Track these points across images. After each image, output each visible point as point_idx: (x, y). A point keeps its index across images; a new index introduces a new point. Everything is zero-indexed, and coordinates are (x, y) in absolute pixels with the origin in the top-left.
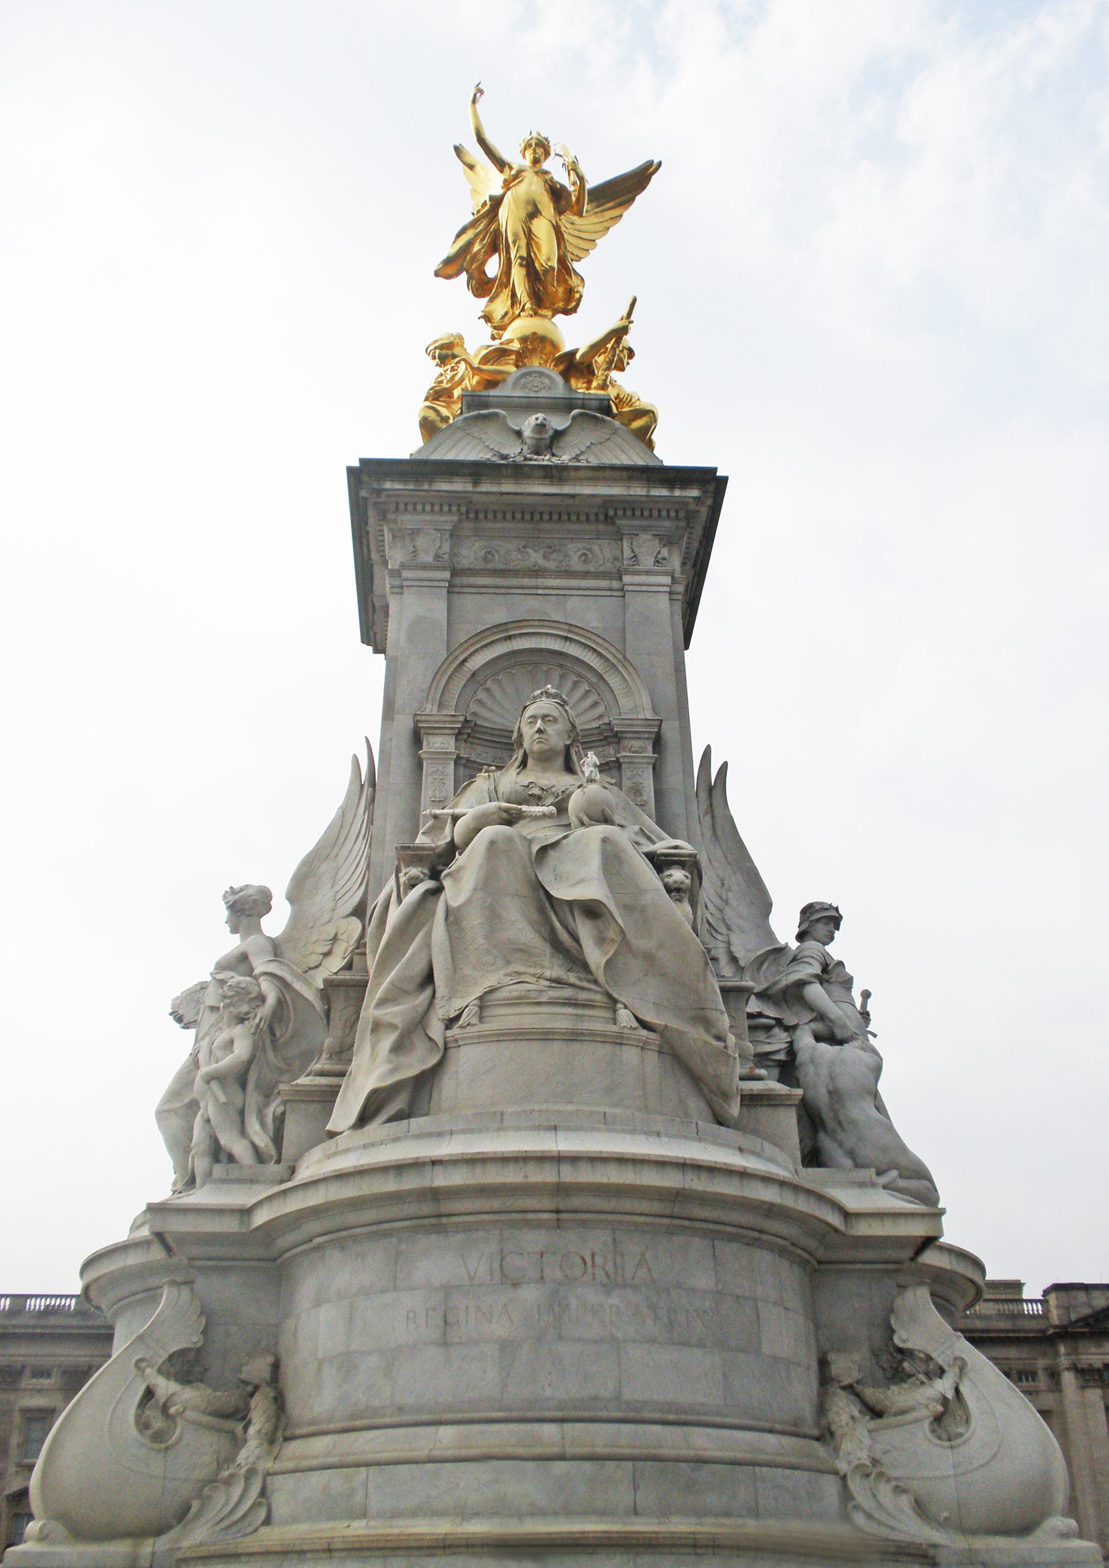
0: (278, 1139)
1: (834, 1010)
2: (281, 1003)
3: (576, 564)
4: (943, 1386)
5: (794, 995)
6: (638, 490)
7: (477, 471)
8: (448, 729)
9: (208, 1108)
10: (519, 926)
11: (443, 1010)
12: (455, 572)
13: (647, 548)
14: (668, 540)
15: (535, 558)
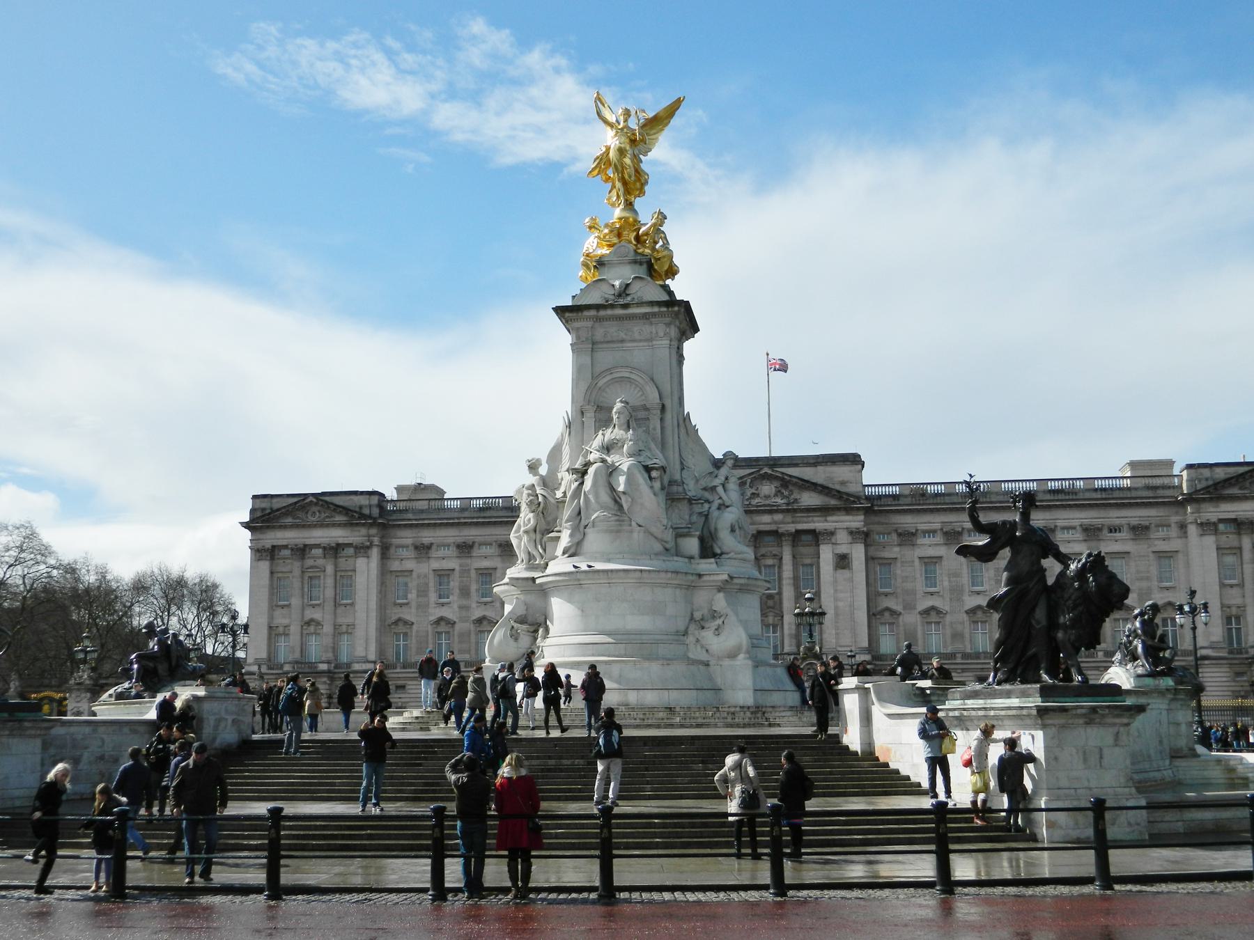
0: (545, 550)
1: (725, 497)
2: (545, 503)
3: (637, 336)
4: (719, 621)
5: (713, 489)
6: (656, 309)
7: (598, 307)
8: (591, 408)
9: (525, 538)
10: (605, 497)
11: (584, 522)
12: (593, 343)
13: (661, 329)
14: (668, 325)
15: (622, 335)
